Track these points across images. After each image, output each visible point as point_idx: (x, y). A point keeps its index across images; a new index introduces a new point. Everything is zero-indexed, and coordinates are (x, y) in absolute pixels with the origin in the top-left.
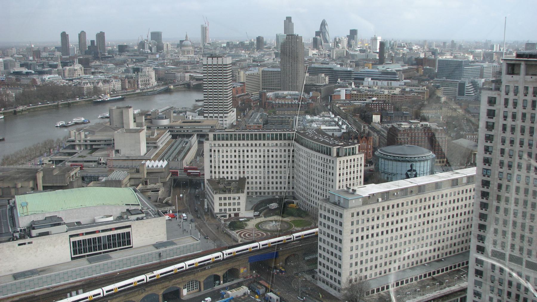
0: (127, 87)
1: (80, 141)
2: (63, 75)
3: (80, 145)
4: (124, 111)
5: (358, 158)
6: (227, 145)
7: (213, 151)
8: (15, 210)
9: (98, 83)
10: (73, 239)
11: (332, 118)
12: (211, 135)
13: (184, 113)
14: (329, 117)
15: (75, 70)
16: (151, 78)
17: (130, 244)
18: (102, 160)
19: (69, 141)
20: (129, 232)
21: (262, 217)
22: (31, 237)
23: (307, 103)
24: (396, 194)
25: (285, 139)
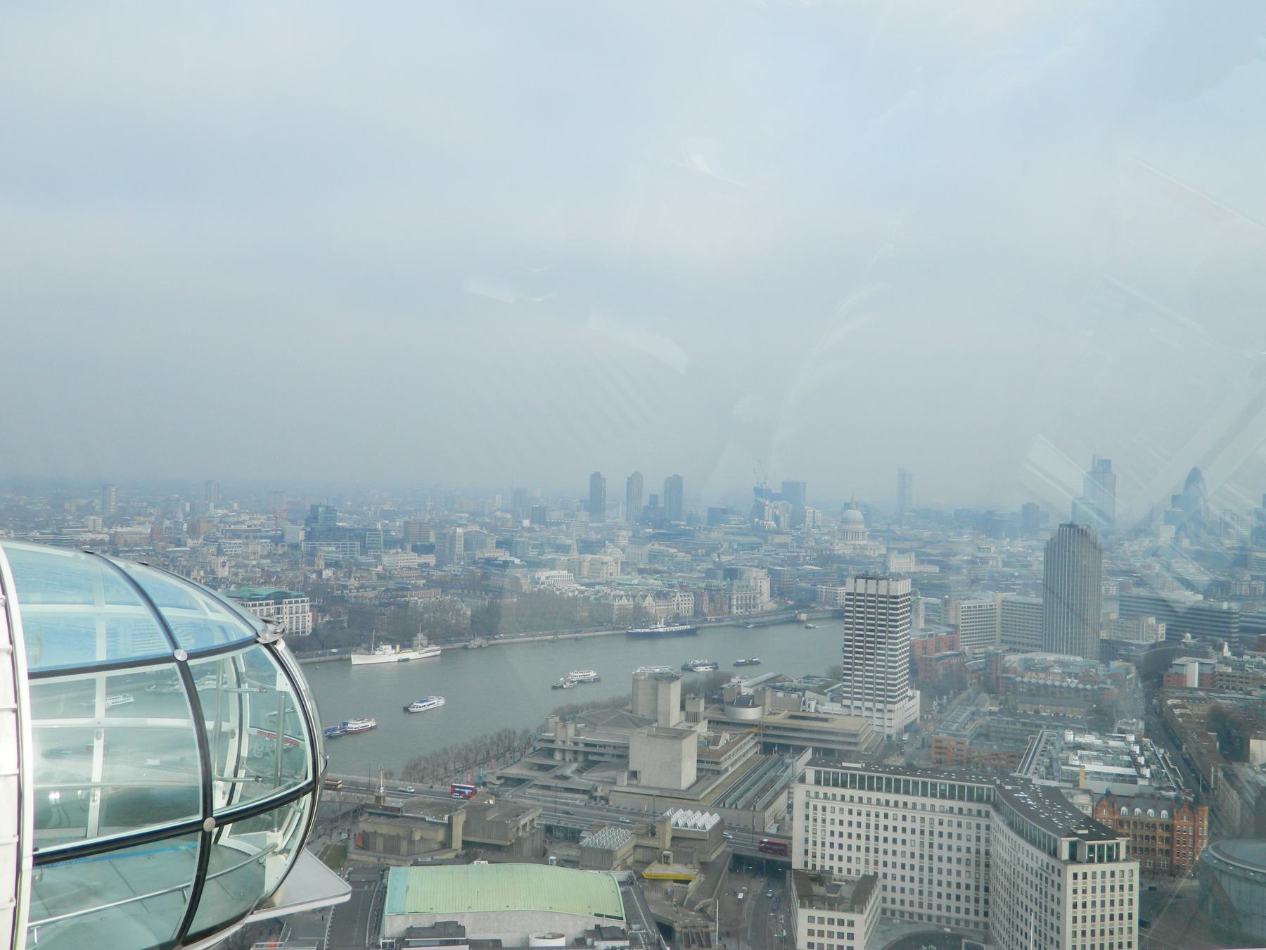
0: (706, 610)
2: (577, 572)
3: (563, 751)
4: (661, 687)
5: (1123, 871)
6: (843, 798)
11: (1129, 743)
12: (811, 775)
13: (801, 693)
14: (1123, 739)
15: (602, 563)
16: (761, 594)
18: (599, 790)
19: (541, 740)
23: (1100, 689)
25: (971, 799)
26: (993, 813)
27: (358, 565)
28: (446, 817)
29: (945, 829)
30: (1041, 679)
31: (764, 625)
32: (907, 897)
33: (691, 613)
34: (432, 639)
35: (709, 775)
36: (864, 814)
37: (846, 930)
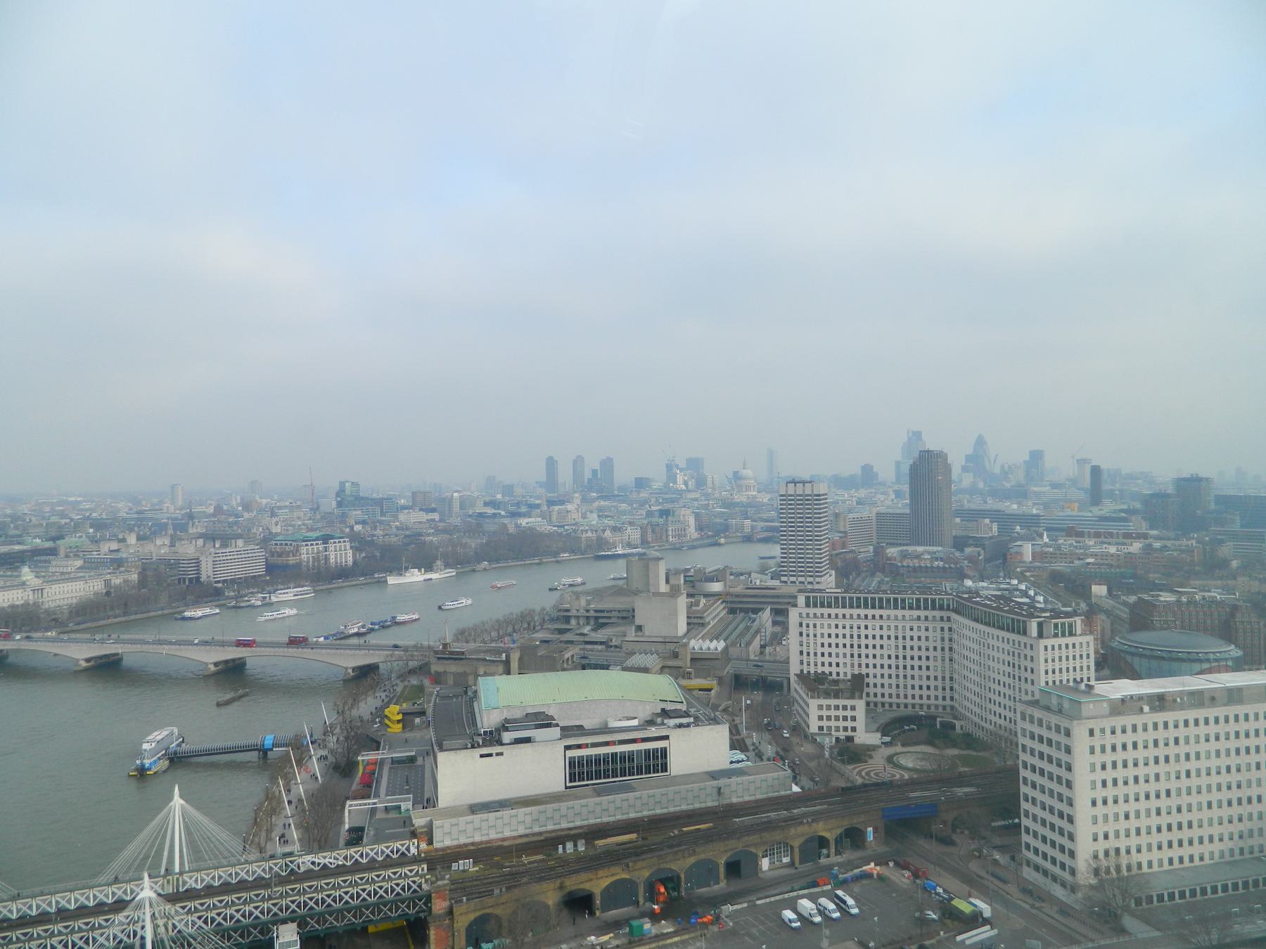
0: (650, 539)
1: (578, 611)
3: (577, 617)
6: (829, 616)
7: (804, 625)
8: (475, 704)
9: (604, 531)
10: (570, 753)
12: (801, 600)
14: (1009, 583)
16: (689, 527)
17: (666, 771)
19: (560, 610)
20: (666, 748)
21: (897, 745)
22: (502, 744)
24: (1179, 700)
25: (934, 608)
26: (954, 616)
27: (381, 522)
28: (504, 655)
29: (915, 634)
30: (916, 563)
31: (694, 547)
32: (887, 691)
33: (639, 542)
34: (447, 565)
35: (696, 627)
36: (848, 627)
37: (849, 713)
